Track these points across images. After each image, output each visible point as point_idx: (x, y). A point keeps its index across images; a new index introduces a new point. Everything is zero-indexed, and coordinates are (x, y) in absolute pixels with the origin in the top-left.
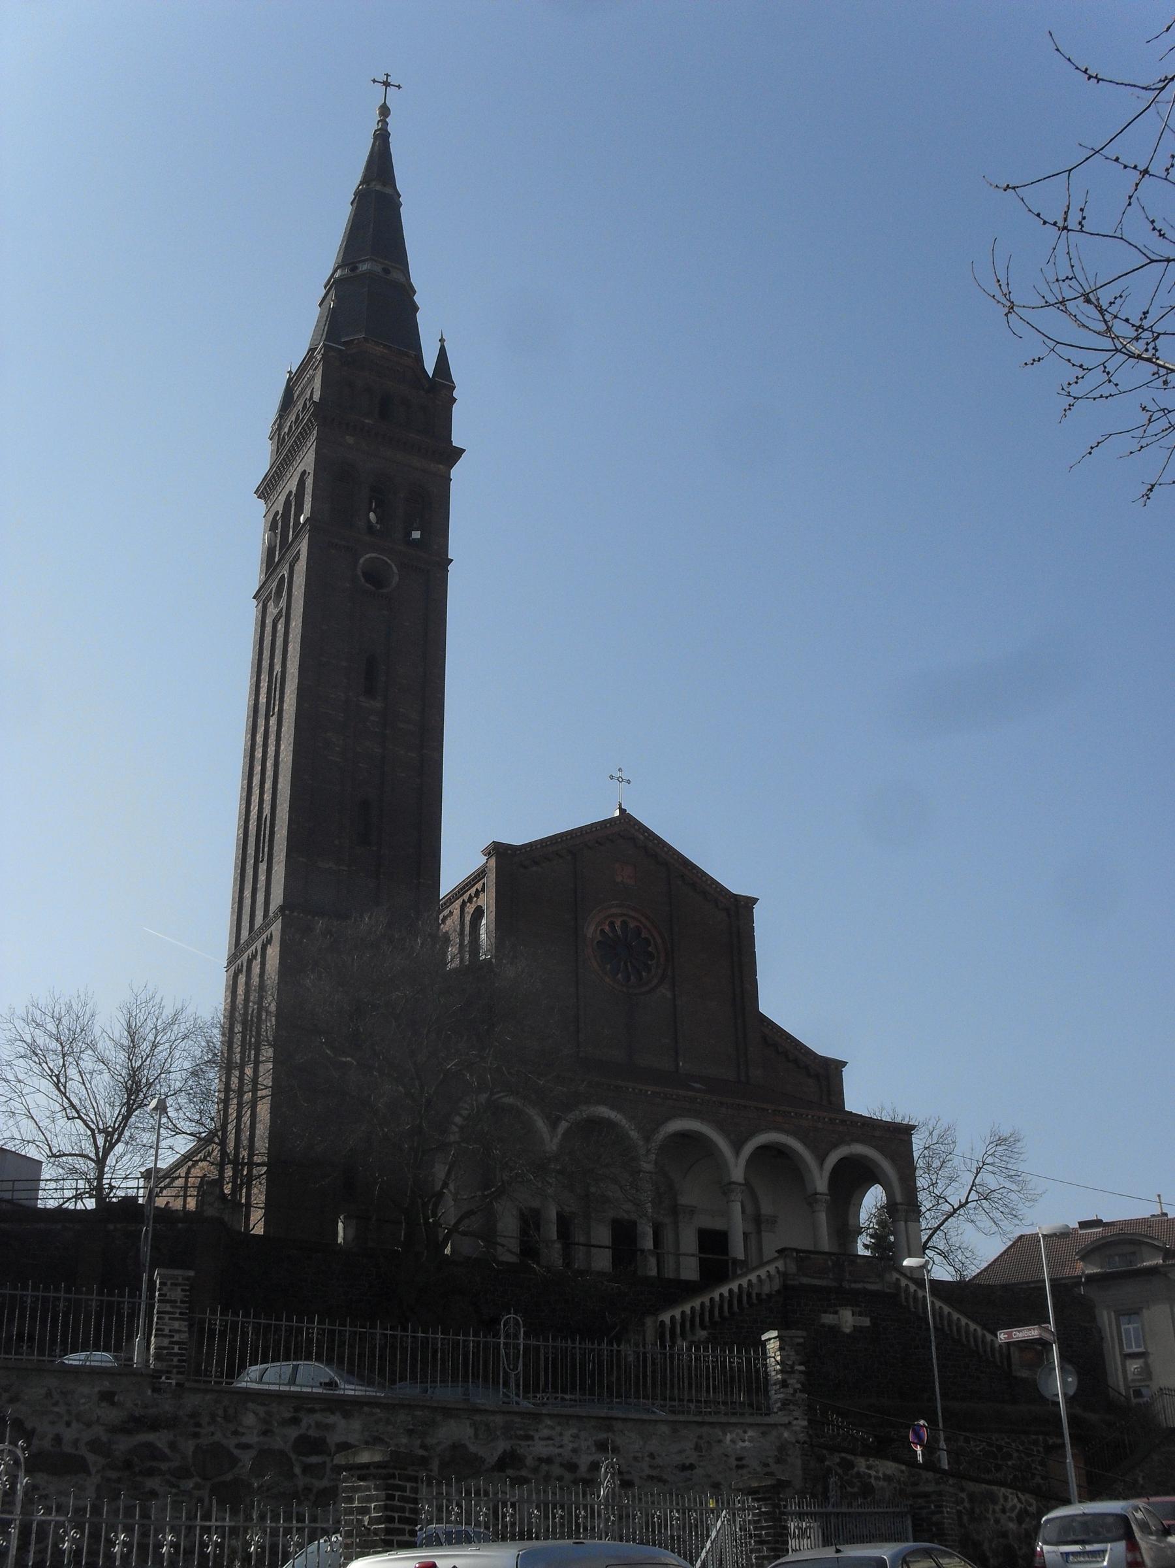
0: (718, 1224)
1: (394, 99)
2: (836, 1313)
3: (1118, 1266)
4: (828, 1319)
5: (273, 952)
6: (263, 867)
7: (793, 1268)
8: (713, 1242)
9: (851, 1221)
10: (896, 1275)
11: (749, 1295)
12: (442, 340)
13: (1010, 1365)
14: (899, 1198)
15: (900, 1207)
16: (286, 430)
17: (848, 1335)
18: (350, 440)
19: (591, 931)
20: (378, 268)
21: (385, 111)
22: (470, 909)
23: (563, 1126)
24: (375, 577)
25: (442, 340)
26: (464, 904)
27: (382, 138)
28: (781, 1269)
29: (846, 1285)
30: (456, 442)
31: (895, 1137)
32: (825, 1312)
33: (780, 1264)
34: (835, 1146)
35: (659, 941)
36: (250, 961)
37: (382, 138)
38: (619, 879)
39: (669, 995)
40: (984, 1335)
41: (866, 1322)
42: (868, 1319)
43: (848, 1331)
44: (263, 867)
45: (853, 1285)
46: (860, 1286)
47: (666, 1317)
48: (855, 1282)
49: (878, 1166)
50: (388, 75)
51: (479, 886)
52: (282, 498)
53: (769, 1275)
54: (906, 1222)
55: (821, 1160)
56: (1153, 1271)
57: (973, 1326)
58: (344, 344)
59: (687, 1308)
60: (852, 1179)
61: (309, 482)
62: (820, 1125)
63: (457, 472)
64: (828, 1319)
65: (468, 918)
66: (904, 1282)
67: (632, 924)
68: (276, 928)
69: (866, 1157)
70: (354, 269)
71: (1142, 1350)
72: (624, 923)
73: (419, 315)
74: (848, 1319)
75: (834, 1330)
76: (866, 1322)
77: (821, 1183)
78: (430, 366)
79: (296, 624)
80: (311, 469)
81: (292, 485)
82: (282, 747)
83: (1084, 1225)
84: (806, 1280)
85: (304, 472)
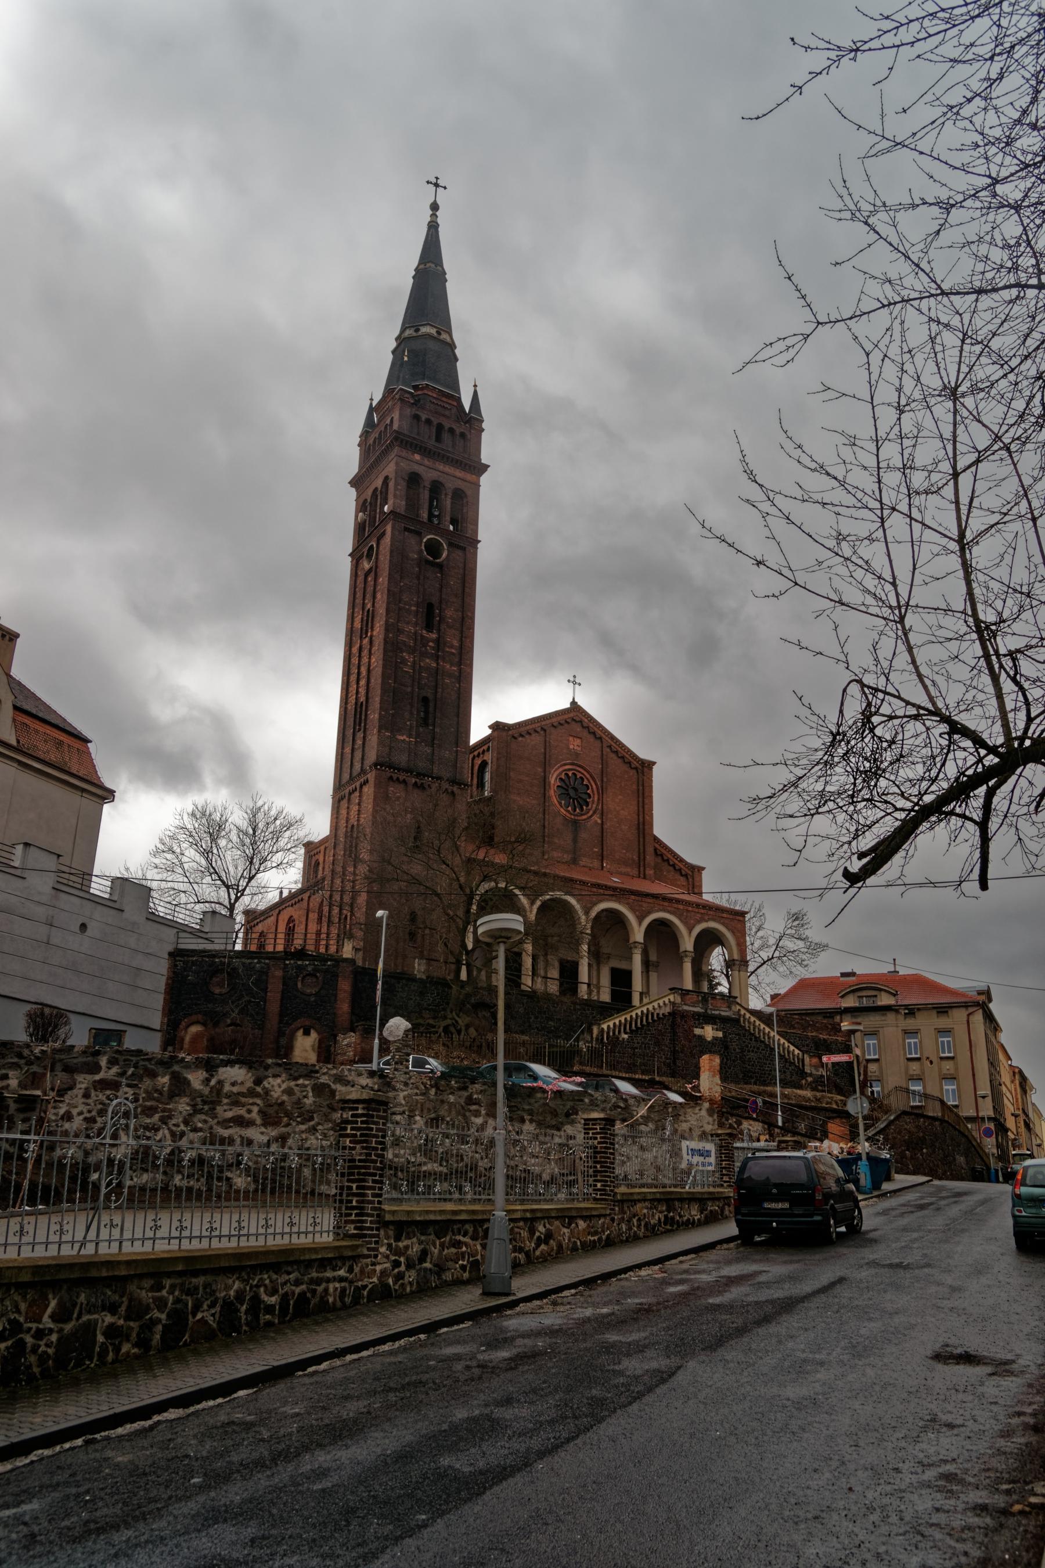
0: (623, 965)
1: (442, 197)
3: (865, 1002)
4: (698, 1031)
5: (369, 790)
6: (360, 735)
7: (678, 1000)
8: (621, 979)
9: (704, 968)
10: (738, 1007)
11: (652, 1014)
12: (475, 386)
13: (803, 1065)
14: (736, 957)
16: (371, 442)
18: (417, 457)
19: (553, 779)
20: (433, 331)
21: (435, 207)
22: (478, 762)
23: (538, 903)
24: (433, 549)
25: (475, 386)
26: (474, 757)
27: (433, 227)
28: (672, 1000)
30: (484, 460)
31: (736, 918)
33: (671, 997)
34: (699, 922)
36: (350, 794)
37: (433, 227)
38: (571, 747)
39: (599, 821)
41: (720, 1034)
44: (360, 735)
46: (717, 1012)
47: (605, 1026)
50: (437, 178)
51: (485, 747)
52: (370, 492)
53: (665, 1004)
55: (690, 931)
56: (887, 1008)
58: (415, 388)
59: (617, 1021)
60: (707, 941)
61: (391, 484)
63: (484, 479)
64: (698, 1031)
65: (476, 768)
66: (743, 1012)
67: (579, 775)
68: (371, 776)
69: (717, 929)
70: (417, 330)
71: (877, 1057)
72: (574, 774)
73: (458, 364)
75: (701, 1038)
76: (720, 1034)
77: (688, 943)
78: (467, 405)
79: (383, 580)
80: (392, 476)
81: (379, 483)
82: (373, 660)
83: (843, 975)
84: (686, 1008)
85: (387, 478)
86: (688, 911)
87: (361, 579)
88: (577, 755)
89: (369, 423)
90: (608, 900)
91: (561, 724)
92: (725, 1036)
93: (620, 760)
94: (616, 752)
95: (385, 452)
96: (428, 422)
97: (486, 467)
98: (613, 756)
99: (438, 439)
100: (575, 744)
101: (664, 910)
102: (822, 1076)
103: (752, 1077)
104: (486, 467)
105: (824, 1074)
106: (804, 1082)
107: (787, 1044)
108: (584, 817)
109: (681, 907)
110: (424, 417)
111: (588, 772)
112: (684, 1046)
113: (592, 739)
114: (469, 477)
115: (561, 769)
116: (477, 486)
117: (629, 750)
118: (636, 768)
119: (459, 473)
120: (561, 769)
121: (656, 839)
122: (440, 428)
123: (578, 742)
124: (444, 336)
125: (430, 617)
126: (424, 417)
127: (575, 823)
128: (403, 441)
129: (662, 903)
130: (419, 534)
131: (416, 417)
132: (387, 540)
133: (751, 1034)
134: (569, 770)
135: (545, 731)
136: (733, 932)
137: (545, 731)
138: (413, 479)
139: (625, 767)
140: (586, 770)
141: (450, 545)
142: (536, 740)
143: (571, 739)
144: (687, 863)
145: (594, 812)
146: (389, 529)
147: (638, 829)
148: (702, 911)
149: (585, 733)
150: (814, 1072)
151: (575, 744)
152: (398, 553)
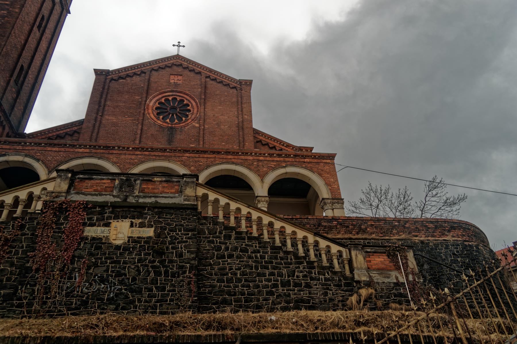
2: (108, 225)
7: (64, 186)
13: (352, 270)
15: (326, 201)
17: (118, 247)
29: (131, 200)
32: (92, 225)
34: (274, 169)
35: (194, 104)
38: (172, 81)
39: (197, 125)
40: (316, 244)
41: (150, 232)
42: (153, 229)
43: (118, 242)
45: (141, 200)
46: (153, 200)
48: (145, 197)
49: (310, 179)
54: (333, 210)
57: (301, 234)
62: (261, 158)
64: (91, 232)
74: (120, 231)
76: (150, 232)
86: (259, 160)
88: (176, 85)
90: (154, 160)
91: (162, 68)
92: (158, 235)
93: (219, 85)
94: (215, 80)
98: (214, 83)
100: (174, 80)
101: (228, 163)
102: (398, 284)
103: (225, 302)
105: (402, 279)
106: (354, 299)
107: (311, 239)
108: (181, 125)
109: (251, 158)
111: (187, 95)
112: (46, 258)
113: (192, 74)
115: (160, 96)
117: (227, 76)
118: (235, 87)
120: (160, 96)
121: (256, 132)
123: (180, 78)
127: (171, 128)
129: (225, 156)
133: (227, 228)
134: (169, 96)
135: (145, 73)
136: (320, 175)
137: (145, 73)
139: (225, 88)
140: (185, 94)
142: (136, 79)
143: (172, 77)
144: (293, 147)
145: (193, 120)
147: (238, 127)
148: (278, 159)
149: (187, 72)
150: (377, 277)
151: (174, 80)
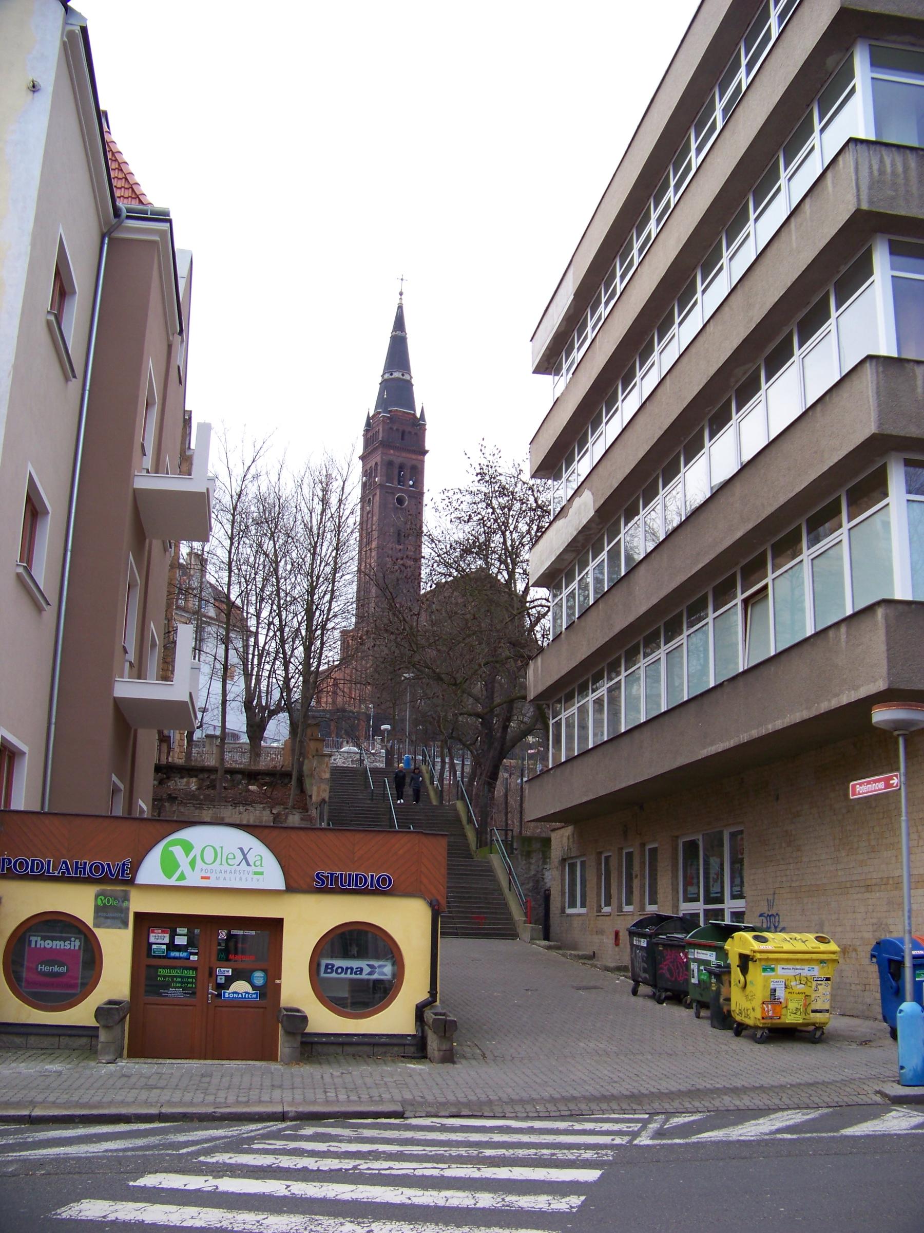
18: (392, 452)
21: (401, 294)
24: (400, 501)
27: (400, 307)
37: (400, 307)
58: (390, 411)
63: (427, 458)
78: (418, 415)
87: (365, 515)
89: (368, 424)
95: (375, 449)
96: (397, 430)
97: (427, 452)
99: (403, 439)
104: (427, 452)
110: (395, 428)
114: (420, 457)
116: (423, 462)
119: (414, 457)
122: (403, 433)
124: (407, 377)
125: (400, 537)
126: (395, 428)
128: (386, 445)
130: (394, 494)
131: (391, 428)
132: (377, 498)
138: (390, 464)
141: (409, 497)
146: (378, 492)
152: (383, 506)
